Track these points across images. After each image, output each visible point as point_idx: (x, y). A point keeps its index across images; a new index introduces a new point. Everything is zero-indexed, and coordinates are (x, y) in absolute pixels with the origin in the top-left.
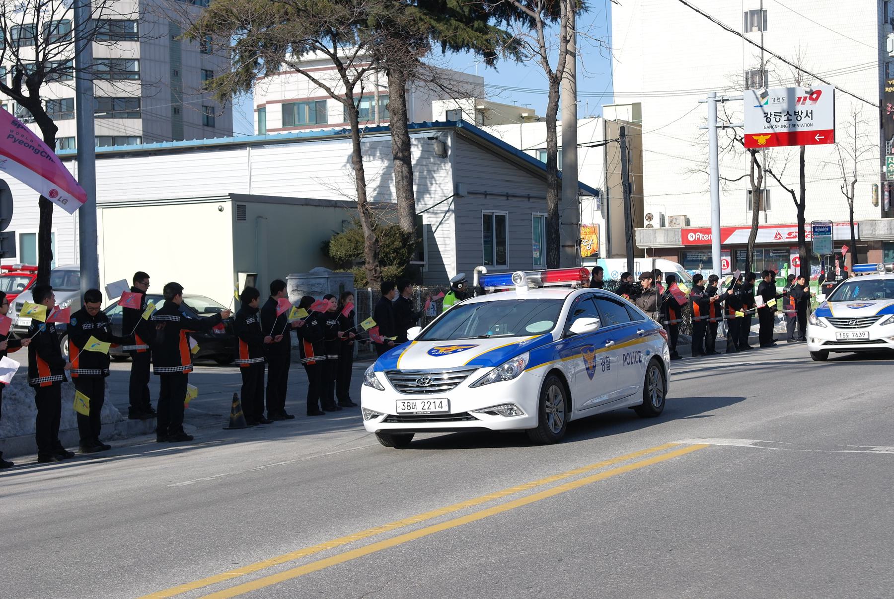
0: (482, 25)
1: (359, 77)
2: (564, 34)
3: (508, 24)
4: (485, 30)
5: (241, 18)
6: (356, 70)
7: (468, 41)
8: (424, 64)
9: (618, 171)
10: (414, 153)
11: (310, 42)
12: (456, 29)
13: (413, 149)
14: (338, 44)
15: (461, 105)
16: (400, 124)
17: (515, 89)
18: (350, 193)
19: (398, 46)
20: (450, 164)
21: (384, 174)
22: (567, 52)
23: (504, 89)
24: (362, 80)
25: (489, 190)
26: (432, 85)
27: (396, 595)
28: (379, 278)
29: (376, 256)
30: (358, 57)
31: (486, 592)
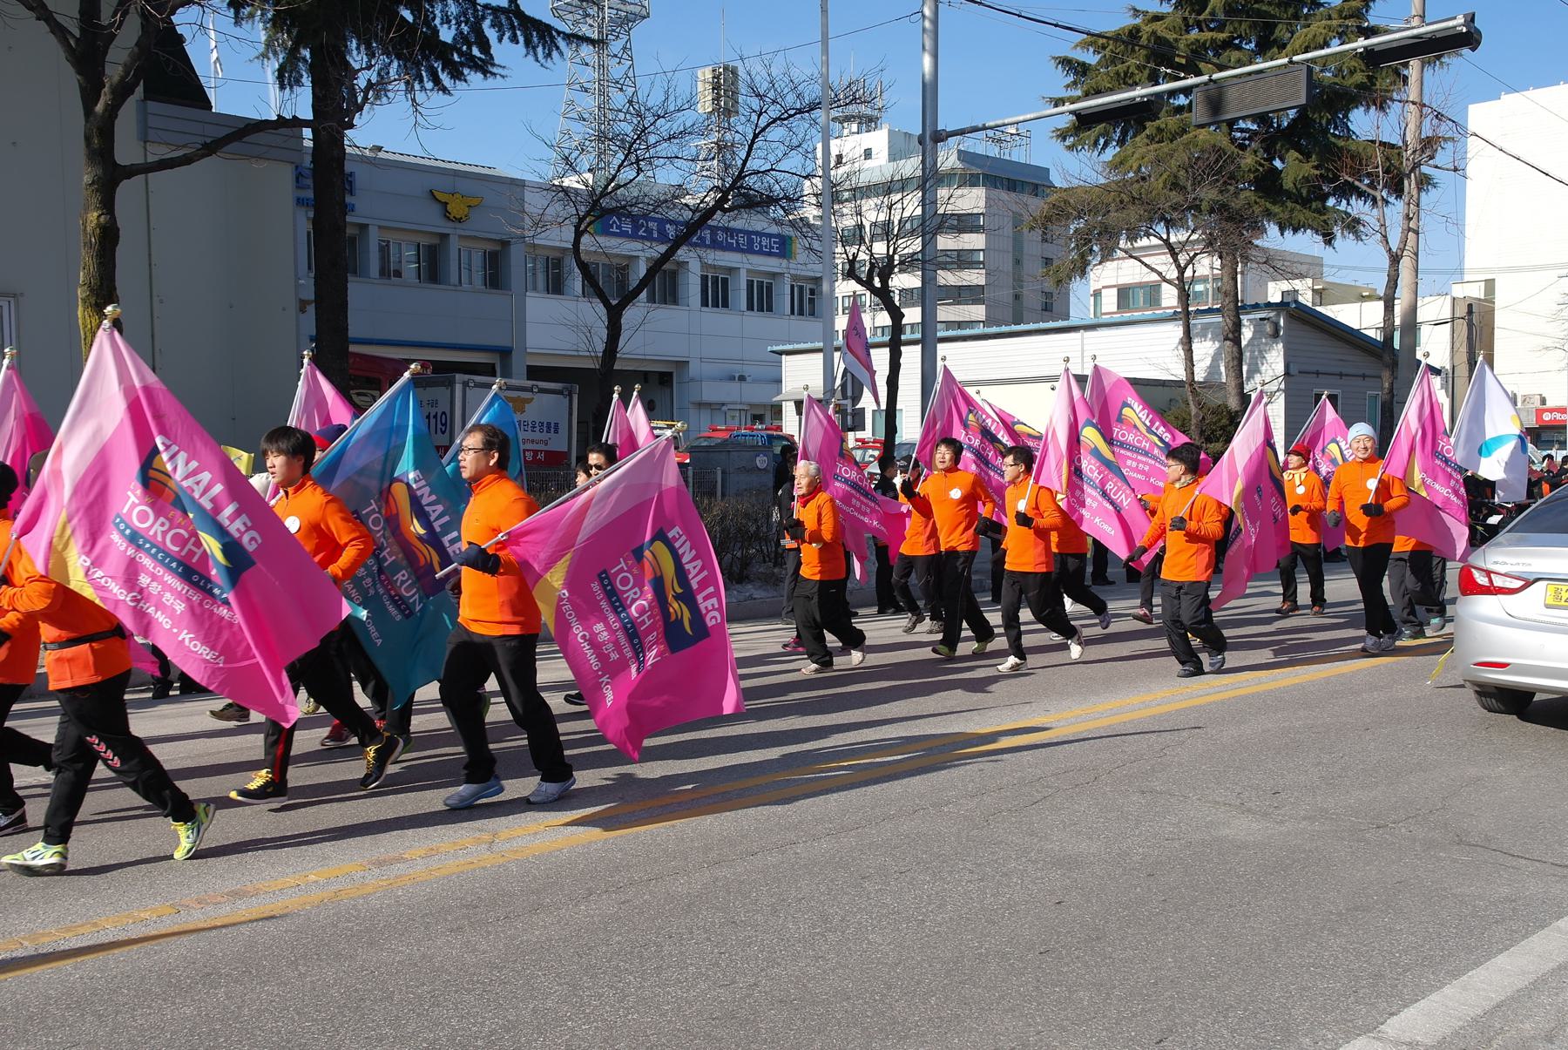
0: (1320, 206)
1: (1191, 260)
2: (1406, 212)
3: (1348, 204)
4: (1323, 210)
8: (1257, 246)
9: (1464, 349)
12: (1292, 210)
13: (1244, 330)
16: (1232, 306)
17: (1354, 268)
18: (1179, 373)
22: (1409, 229)
23: (1340, 268)
25: (1321, 369)
26: (1265, 267)
29: (1202, 432)
30: (1191, 242)
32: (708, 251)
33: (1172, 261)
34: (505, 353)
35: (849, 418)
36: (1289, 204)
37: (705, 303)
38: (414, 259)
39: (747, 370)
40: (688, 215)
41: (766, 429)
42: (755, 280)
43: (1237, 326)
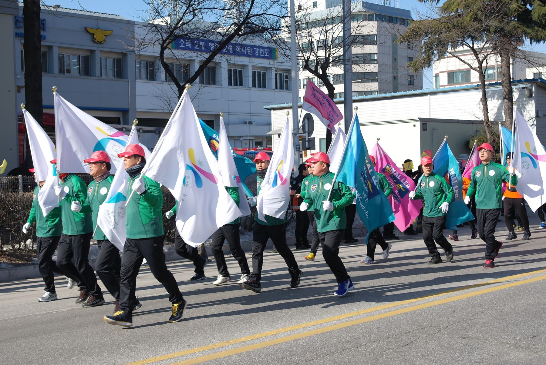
1: (485, 58)
5: (425, 31)
6: (484, 54)
7: (544, 37)
8: (520, 50)
10: (515, 95)
11: (460, 41)
12: (537, 31)
14: (474, 42)
15: (539, 70)
16: (507, 81)
18: (480, 117)
19: (506, 41)
20: (534, 101)
21: (499, 106)
24: (487, 60)
26: (524, 61)
27: (492, 315)
28: (495, 159)
30: (485, 48)
31: (539, 316)
32: (231, 57)
33: (475, 58)
34: (125, 112)
35: (307, 143)
36: (536, 28)
37: (230, 84)
38: (77, 63)
39: (253, 119)
40: (220, 38)
41: (263, 149)
42: (257, 71)
43: (511, 92)
